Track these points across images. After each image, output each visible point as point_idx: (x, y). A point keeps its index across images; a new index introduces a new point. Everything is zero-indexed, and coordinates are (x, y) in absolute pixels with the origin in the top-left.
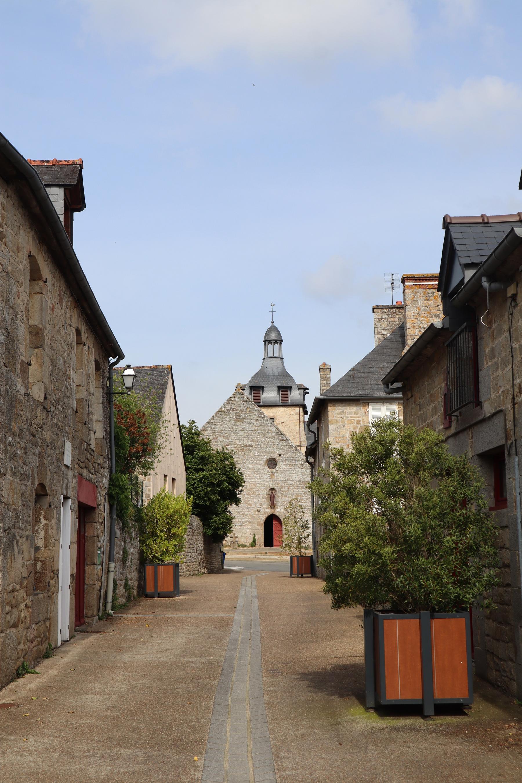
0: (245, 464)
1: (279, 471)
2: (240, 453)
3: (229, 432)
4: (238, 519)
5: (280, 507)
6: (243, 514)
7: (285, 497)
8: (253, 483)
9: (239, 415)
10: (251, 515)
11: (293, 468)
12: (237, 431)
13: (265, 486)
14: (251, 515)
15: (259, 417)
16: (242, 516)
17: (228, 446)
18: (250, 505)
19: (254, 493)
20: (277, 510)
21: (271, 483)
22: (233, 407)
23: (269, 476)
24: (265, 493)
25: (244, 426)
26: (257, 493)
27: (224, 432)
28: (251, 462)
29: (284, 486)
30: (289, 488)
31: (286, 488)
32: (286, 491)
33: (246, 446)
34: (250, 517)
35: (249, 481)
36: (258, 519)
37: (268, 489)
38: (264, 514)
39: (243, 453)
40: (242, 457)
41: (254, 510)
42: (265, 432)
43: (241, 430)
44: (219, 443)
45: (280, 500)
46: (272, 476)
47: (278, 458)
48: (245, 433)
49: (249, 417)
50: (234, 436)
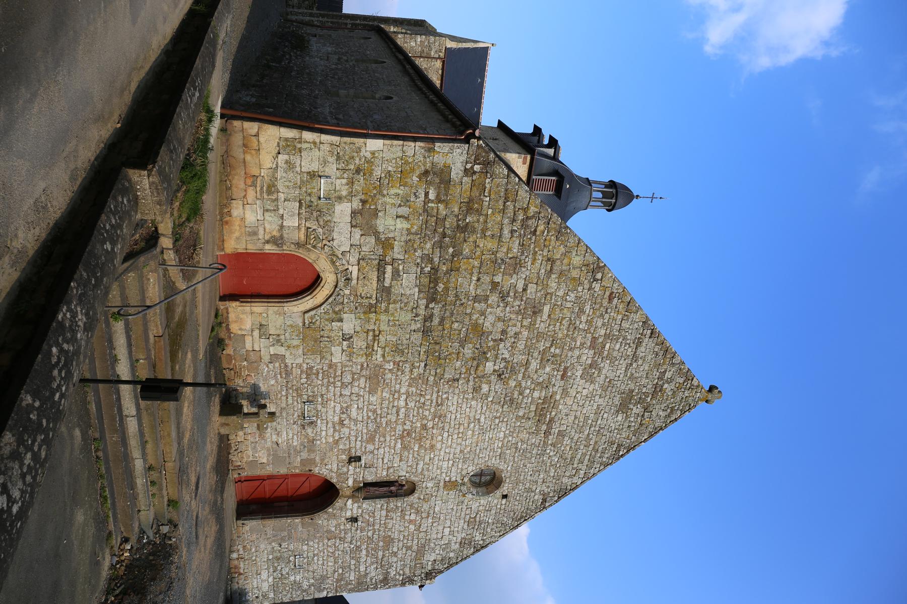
0: (497, 421)
1: (461, 498)
2: (533, 408)
3: (603, 377)
4: (324, 410)
5: (359, 507)
6: (341, 422)
7: (387, 516)
8: (439, 446)
9: (640, 401)
10: (336, 442)
11: (466, 527)
12: (597, 397)
13: (426, 473)
14: (336, 442)
15: (619, 446)
16: (336, 419)
17: (562, 379)
18: (371, 440)
19: (405, 447)
20: (350, 502)
21: (430, 485)
22: (666, 386)
23: (453, 479)
24: (402, 472)
25: (606, 415)
26: (406, 453)
27: (606, 366)
28: (502, 435)
29: (418, 512)
30: (411, 522)
31: (413, 517)
32: (403, 516)
33: (550, 421)
34: (331, 440)
35: (446, 435)
36: (322, 460)
37: (413, 478)
38: (339, 475)
39: (533, 414)
40: (521, 414)
41: (353, 451)
42: (576, 462)
43: (598, 408)
44: (577, 352)
45: (379, 506)
46: (451, 485)
47: (498, 493)
48: (587, 418)
49: (626, 425)
50: (585, 392)
